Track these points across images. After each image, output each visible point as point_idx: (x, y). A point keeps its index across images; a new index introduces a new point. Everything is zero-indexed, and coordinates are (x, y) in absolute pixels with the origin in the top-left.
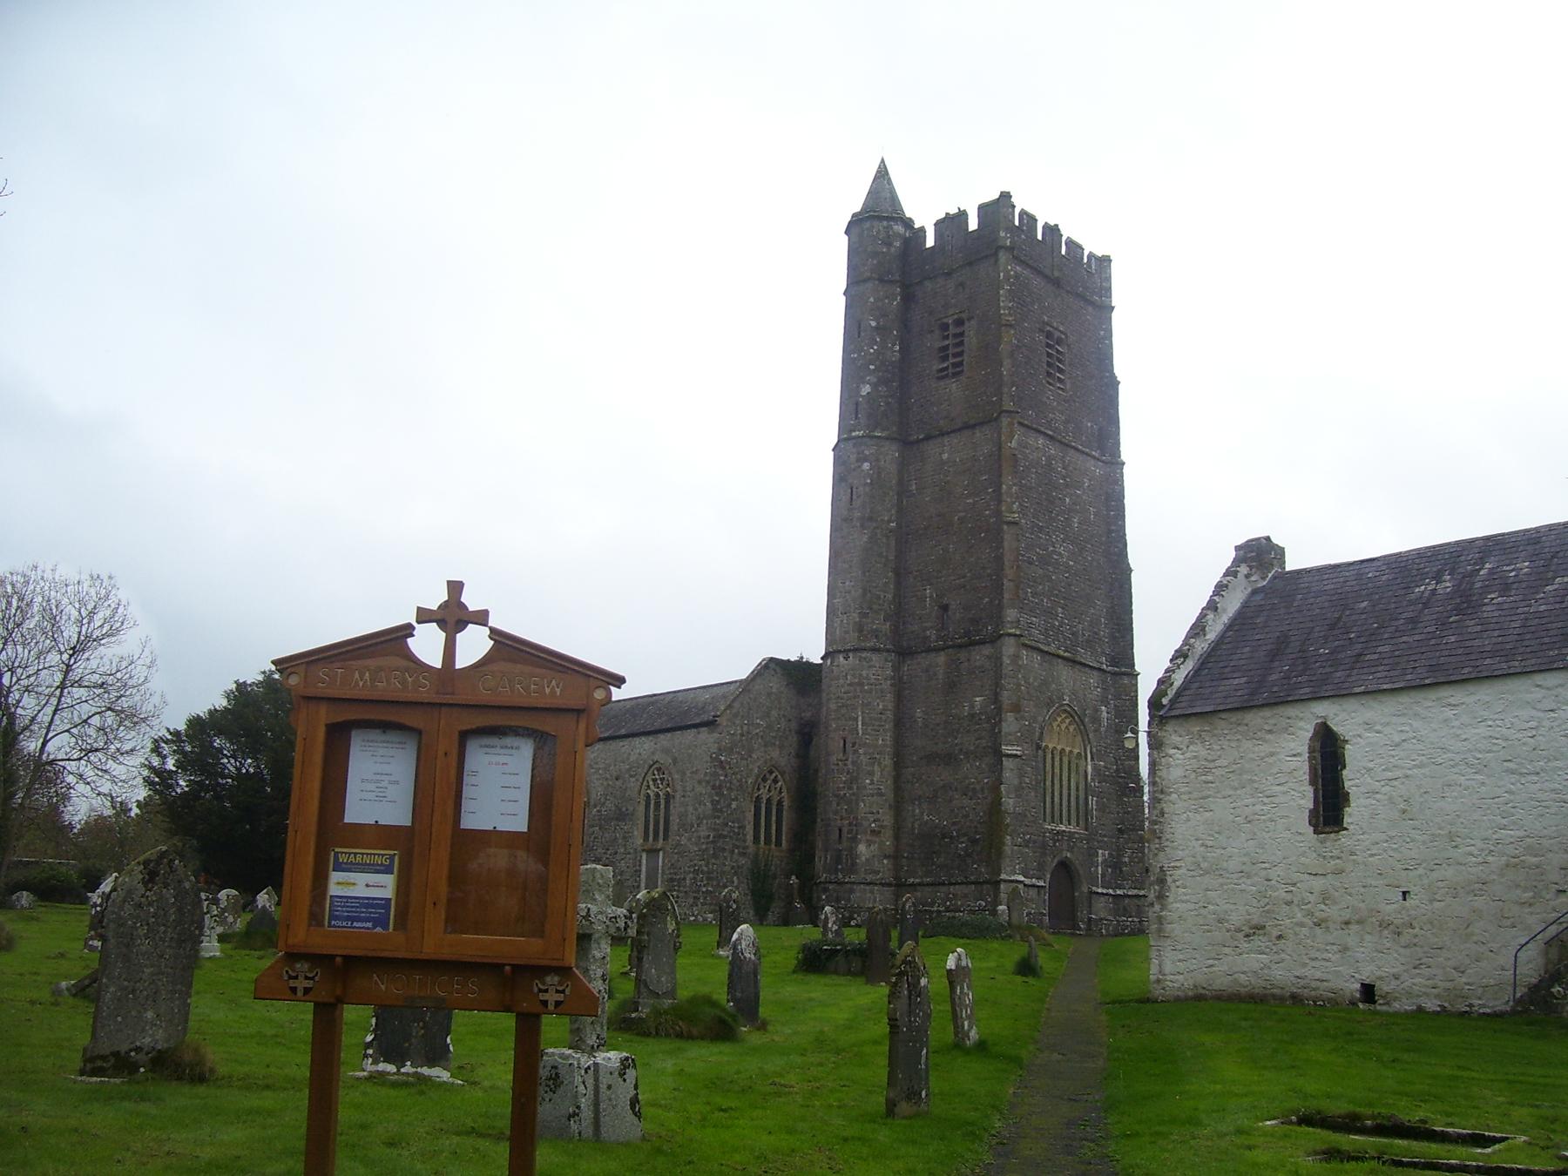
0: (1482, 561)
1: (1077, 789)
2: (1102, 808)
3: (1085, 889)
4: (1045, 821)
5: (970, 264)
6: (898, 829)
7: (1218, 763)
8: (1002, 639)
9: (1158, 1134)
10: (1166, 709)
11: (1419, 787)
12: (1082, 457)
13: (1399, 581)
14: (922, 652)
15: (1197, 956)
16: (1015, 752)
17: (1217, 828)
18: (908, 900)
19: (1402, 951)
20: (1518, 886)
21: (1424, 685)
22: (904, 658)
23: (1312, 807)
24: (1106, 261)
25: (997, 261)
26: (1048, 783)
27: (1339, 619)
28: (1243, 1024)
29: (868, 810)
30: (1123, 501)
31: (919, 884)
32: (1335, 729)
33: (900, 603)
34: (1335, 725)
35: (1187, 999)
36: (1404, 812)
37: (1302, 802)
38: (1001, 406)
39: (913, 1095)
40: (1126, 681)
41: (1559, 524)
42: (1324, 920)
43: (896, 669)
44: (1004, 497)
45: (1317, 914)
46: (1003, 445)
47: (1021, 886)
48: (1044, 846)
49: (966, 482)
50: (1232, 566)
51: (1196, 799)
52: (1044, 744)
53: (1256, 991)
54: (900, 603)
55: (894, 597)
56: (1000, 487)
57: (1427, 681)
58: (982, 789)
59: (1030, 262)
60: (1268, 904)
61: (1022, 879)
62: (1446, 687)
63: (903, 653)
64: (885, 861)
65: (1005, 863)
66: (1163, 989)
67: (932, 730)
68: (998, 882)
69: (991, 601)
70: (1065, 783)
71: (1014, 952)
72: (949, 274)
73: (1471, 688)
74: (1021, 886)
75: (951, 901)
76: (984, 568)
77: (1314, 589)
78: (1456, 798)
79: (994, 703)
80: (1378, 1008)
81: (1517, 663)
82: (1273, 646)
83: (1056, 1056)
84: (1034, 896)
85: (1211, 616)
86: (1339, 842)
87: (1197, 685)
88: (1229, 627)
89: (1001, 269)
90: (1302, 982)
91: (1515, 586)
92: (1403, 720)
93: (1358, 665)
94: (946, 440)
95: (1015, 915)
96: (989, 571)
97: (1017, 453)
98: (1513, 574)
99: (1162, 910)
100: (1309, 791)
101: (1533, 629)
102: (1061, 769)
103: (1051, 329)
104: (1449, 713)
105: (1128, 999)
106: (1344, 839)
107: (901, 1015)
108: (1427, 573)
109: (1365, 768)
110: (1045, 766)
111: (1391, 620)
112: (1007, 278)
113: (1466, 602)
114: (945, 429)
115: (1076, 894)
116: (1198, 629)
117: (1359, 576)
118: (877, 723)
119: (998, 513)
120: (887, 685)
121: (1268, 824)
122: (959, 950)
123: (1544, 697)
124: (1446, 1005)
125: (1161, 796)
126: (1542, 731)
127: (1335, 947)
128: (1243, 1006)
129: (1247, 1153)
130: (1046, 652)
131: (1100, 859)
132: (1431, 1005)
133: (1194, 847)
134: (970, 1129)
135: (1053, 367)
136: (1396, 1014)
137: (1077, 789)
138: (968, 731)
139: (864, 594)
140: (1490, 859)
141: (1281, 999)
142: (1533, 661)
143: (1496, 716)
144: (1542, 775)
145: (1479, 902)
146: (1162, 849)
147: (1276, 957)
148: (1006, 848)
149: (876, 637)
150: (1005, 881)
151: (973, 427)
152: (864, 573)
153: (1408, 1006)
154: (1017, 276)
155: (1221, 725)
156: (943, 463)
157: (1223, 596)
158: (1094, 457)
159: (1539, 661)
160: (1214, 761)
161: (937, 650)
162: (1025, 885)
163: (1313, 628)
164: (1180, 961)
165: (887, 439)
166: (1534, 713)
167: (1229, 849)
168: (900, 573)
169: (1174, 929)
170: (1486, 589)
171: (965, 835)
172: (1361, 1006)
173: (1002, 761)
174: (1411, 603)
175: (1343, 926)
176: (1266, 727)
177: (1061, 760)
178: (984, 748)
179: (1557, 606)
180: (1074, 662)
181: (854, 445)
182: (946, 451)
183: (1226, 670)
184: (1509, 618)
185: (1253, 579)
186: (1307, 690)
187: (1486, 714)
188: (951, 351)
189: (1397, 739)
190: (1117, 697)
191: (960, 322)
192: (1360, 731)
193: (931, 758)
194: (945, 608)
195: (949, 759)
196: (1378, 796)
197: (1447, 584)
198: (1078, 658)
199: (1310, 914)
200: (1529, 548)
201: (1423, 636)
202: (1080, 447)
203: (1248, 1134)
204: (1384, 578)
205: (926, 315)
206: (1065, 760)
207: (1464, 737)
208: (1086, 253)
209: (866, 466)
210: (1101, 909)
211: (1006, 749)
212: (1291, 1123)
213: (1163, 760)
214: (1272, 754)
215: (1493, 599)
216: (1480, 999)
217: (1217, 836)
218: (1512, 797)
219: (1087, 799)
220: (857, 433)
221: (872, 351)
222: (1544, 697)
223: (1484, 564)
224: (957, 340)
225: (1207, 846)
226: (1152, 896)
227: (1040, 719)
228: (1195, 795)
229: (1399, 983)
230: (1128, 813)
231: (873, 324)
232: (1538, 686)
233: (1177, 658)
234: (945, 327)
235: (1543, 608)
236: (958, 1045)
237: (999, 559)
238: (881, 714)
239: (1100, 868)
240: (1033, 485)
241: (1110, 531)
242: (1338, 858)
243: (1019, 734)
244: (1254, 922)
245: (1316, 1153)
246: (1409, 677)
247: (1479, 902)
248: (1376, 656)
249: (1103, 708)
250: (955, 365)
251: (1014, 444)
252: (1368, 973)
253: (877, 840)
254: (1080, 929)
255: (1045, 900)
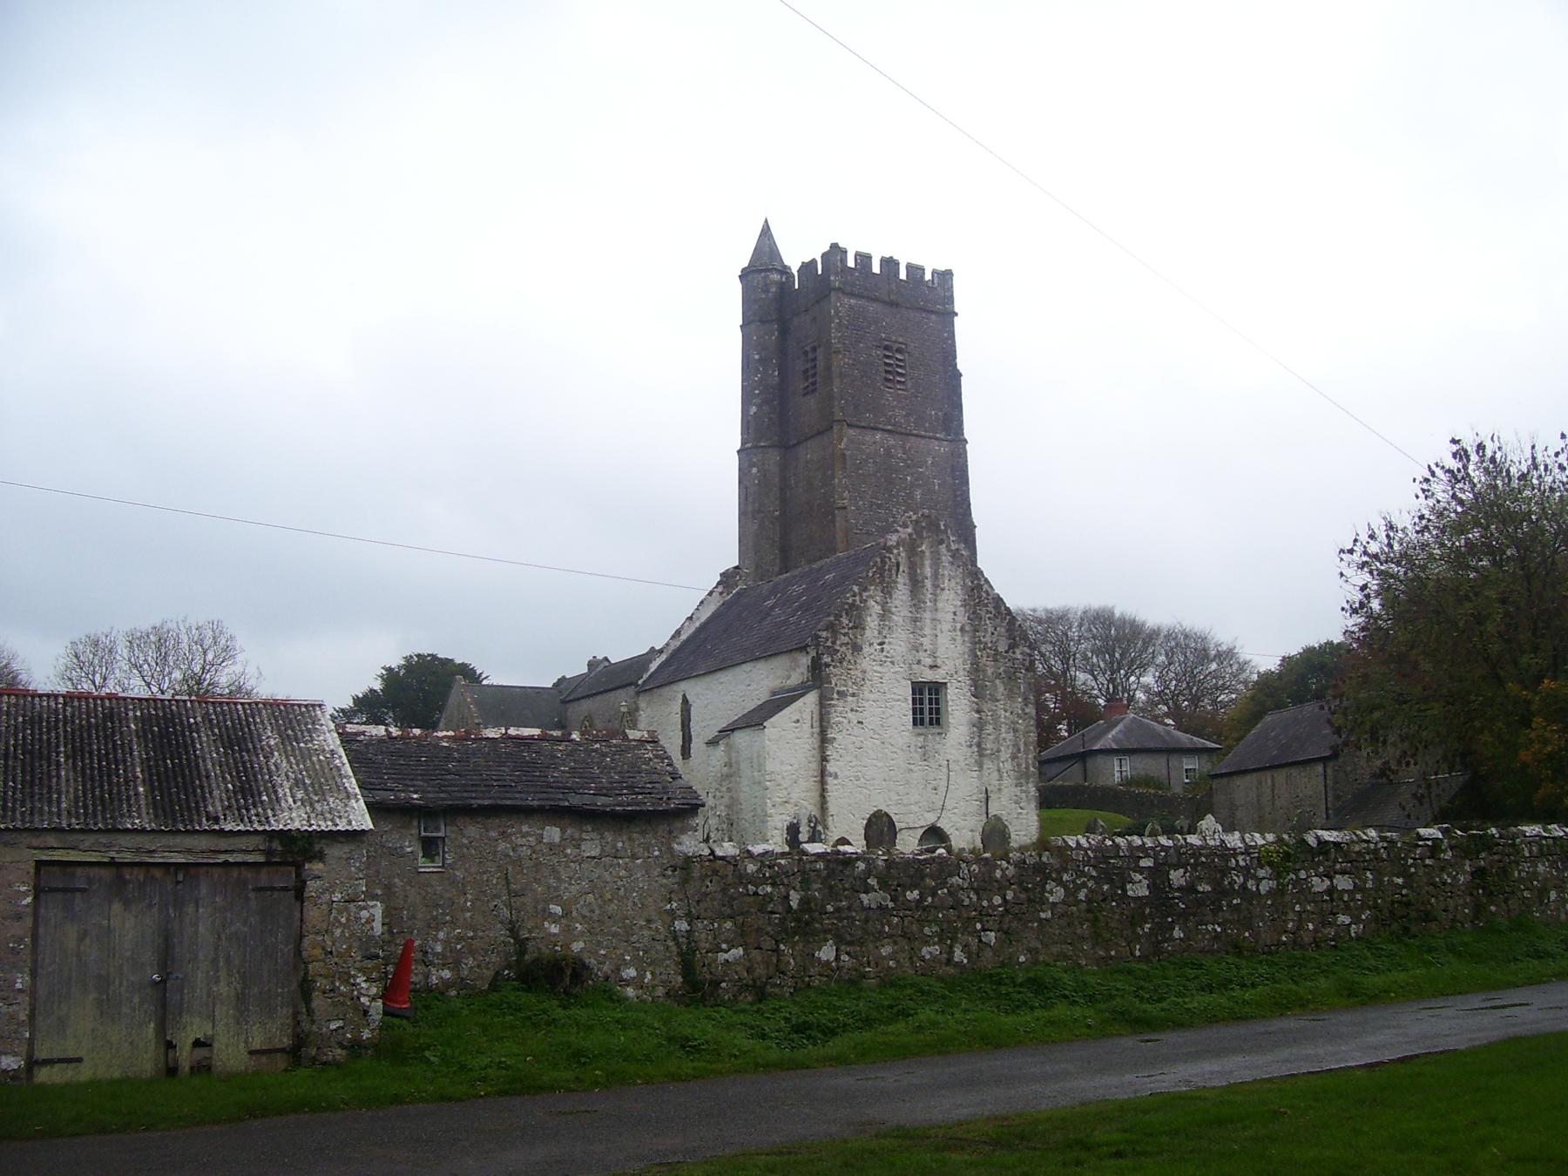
152: (755, 553)
165: (769, 447)
209: (754, 470)
221: (756, 379)
231: (757, 357)
234: (806, 353)
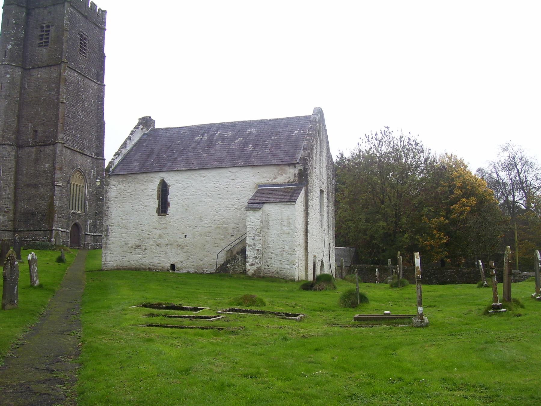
0: (217, 131)
1: (82, 199)
2: (90, 205)
3: (83, 233)
4: (70, 209)
5: (54, 5)
6: (15, 211)
7: (128, 191)
8: (57, 144)
9: (96, 311)
10: (111, 172)
11: (192, 202)
12: (90, 81)
13: (191, 135)
14: (27, 147)
15: (118, 255)
16: (60, 185)
17: (126, 213)
18: (17, 236)
19: (184, 254)
20: (220, 234)
21: (195, 169)
22: (19, 149)
23: (158, 207)
24: (104, 12)
25: (64, 6)
26: (71, 196)
27: (171, 146)
28: (131, 277)
29: (4, 203)
30: (104, 99)
31: (22, 231)
32: (166, 182)
33: (19, 128)
34: (167, 180)
35: (114, 269)
36: (187, 209)
37: (155, 205)
38: (62, 60)
39: (12, 302)
40: (101, 161)
41: (241, 121)
42: (160, 244)
43: (16, 152)
44: (61, 93)
45: (158, 242)
46: (61, 74)
47: (60, 232)
48: (69, 218)
49: (47, 86)
50: (137, 125)
51: (119, 203)
52: (70, 182)
53: (137, 267)
54: (19, 128)
55: (17, 126)
56: (59, 90)
57: (196, 168)
58: (47, 197)
59: (77, 8)
60: (142, 238)
61: (61, 229)
62: (202, 170)
63: (19, 147)
64: (10, 222)
65: (55, 224)
66: (106, 266)
67: (29, 175)
68: (52, 230)
69: (53, 130)
70: (77, 196)
71: (56, 254)
72: (45, 7)
73: (210, 171)
74: (60, 232)
75: (34, 236)
76: (51, 118)
77: (163, 135)
78: (203, 206)
79: (53, 167)
80: (176, 272)
81: (224, 164)
82: (149, 153)
83: (67, 289)
84: (65, 235)
85: (128, 142)
86: (166, 219)
87: (122, 165)
88: (134, 146)
89: (66, 9)
90: (152, 264)
91: (226, 140)
92: (188, 180)
93: (175, 161)
94: (40, 70)
95: (57, 242)
96: (53, 119)
97: (66, 77)
98: (226, 136)
99: (107, 240)
100: (157, 202)
101: (230, 154)
102: (76, 191)
103: (83, 34)
104: (203, 179)
105: (94, 270)
106: (167, 218)
107: (8, 275)
108: (200, 133)
109: (175, 195)
110: (70, 190)
111: (187, 147)
112: (68, 12)
113: (211, 143)
114: (40, 66)
115: (80, 235)
116: (124, 146)
117: (178, 132)
118: (8, 172)
119: (58, 99)
120: (12, 158)
121: (143, 212)
122: (33, 253)
123: (231, 175)
124: (196, 271)
125: (108, 202)
126: (230, 186)
127: (163, 253)
128: (132, 272)
129: (124, 316)
130: (73, 150)
131: (89, 223)
132: (192, 271)
133: (118, 219)
134: (32, 312)
135: (83, 48)
136: (181, 274)
137: (82, 199)
138: (43, 176)
139: (5, 124)
140: (212, 225)
141: (145, 269)
142: (229, 164)
143: (217, 180)
144: (229, 199)
145: (208, 239)
146: (107, 220)
147: (144, 256)
148: (55, 218)
149: (9, 140)
150: (54, 230)
151: (51, 66)
152: (5, 116)
153: (184, 271)
154: (71, 13)
155: (129, 179)
156: (38, 78)
157: (133, 135)
158: (95, 82)
159: (231, 164)
160: (126, 190)
161: (32, 146)
162: (62, 231)
163: (162, 148)
164: (112, 257)
165: (17, 66)
166: (228, 180)
167: (130, 220)
168: (19, 117)
169: (111, 246)
170: (217, 140)
171: (40, 213)
172: (170, 271)
173: (55, 187)
174: (194, 142)
175: (166, 246)
176: (144, 180)
177: (76, 188)
178: (48, 182)
179: (238, 147)
180: (83, 154)
181: (4, 68)
182: (39, 74)
183: (133, 160)
184: (223, 150)
185: (144, 130)
186: (159, 168)
187: (214, 179)
188: (44, 37)
189: (186, 186)
190: (97, 167)
191: (48, 27)
192: (174, 183)
193: (28, 185)
194: (36, 131)
195: (35, 186)
196: (179, 204)
197: (206, 137)
198: (84, 153)
199: (155, 242)
200: (232, 128)
201: (197, 153)
202: (90, 78)
203: (126, 310)
204: (186, 133)
205: (35, 22)
206: (78, 188)
207: (206, 186)
208: (98, 8)
209: (8, 76)
210: (89, 240)
211: (56, 183)
212: (140, 306)
213: (109, 189)
214: (146, 189)
215: (219, 143)
216: (207, 269)
217: (126, 216)
218: (220, 206)
219: (85, 202)
220: (5, 63)
221: (13, 32)
222: (231, 175)
223: (217, 132)
224: (47, 33)
225: (123, 219)
226: (103, 235)
227: (69, 173)
228: (120, 201)
229: (182, 264)
230: (99, 207)
231: (14, 22)
232: (230, 172)
233: (116, 155)
234: (42, 27)
235: (234, 147)
236: (32, 286)
237: (57, 115)
238: (10, 168)
239: (89, 226)
240: (72, 90)
241: (98, 109)
242: (165, 224)
243: (61, 178)
244: (137, 244)
245: (146, 315)
246: (191, 166)
247: (208, 239)
248: (181, 159)
249: (92, 170)
250: (45, 42)
251: (65, 74)
252: (173, 261)
253: (7, 214)
254: (81, 247)
255: (69, 237)
